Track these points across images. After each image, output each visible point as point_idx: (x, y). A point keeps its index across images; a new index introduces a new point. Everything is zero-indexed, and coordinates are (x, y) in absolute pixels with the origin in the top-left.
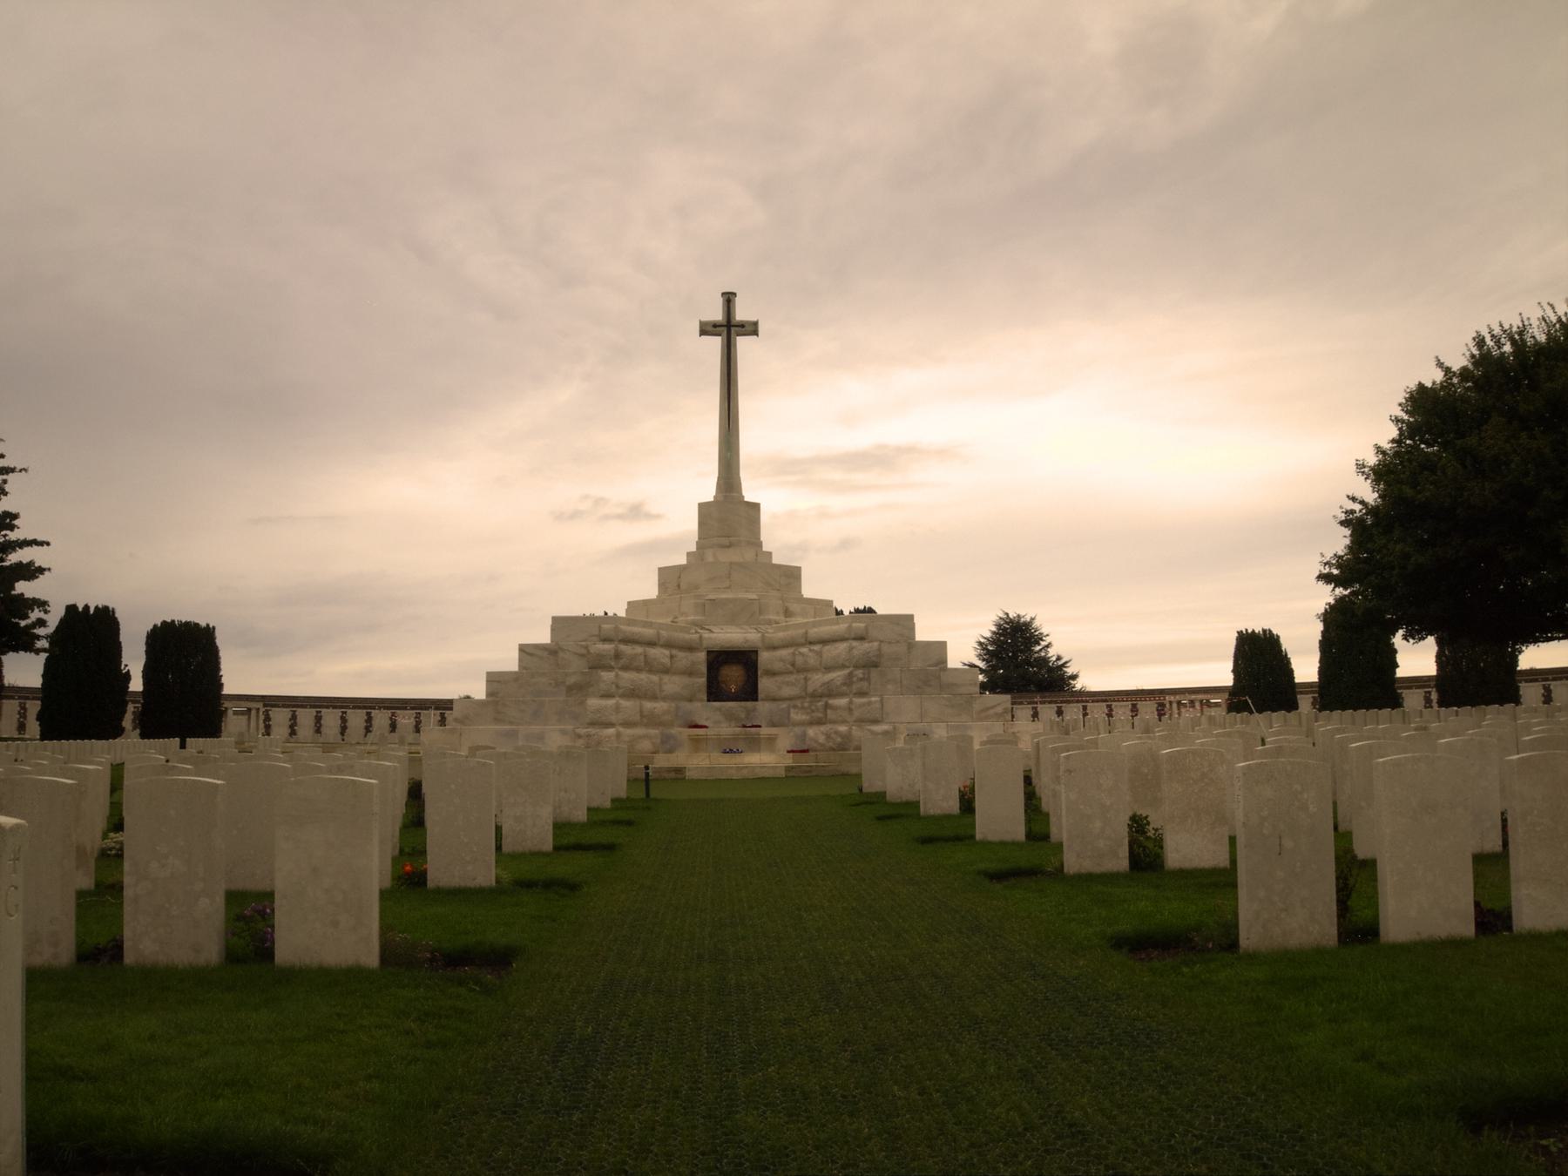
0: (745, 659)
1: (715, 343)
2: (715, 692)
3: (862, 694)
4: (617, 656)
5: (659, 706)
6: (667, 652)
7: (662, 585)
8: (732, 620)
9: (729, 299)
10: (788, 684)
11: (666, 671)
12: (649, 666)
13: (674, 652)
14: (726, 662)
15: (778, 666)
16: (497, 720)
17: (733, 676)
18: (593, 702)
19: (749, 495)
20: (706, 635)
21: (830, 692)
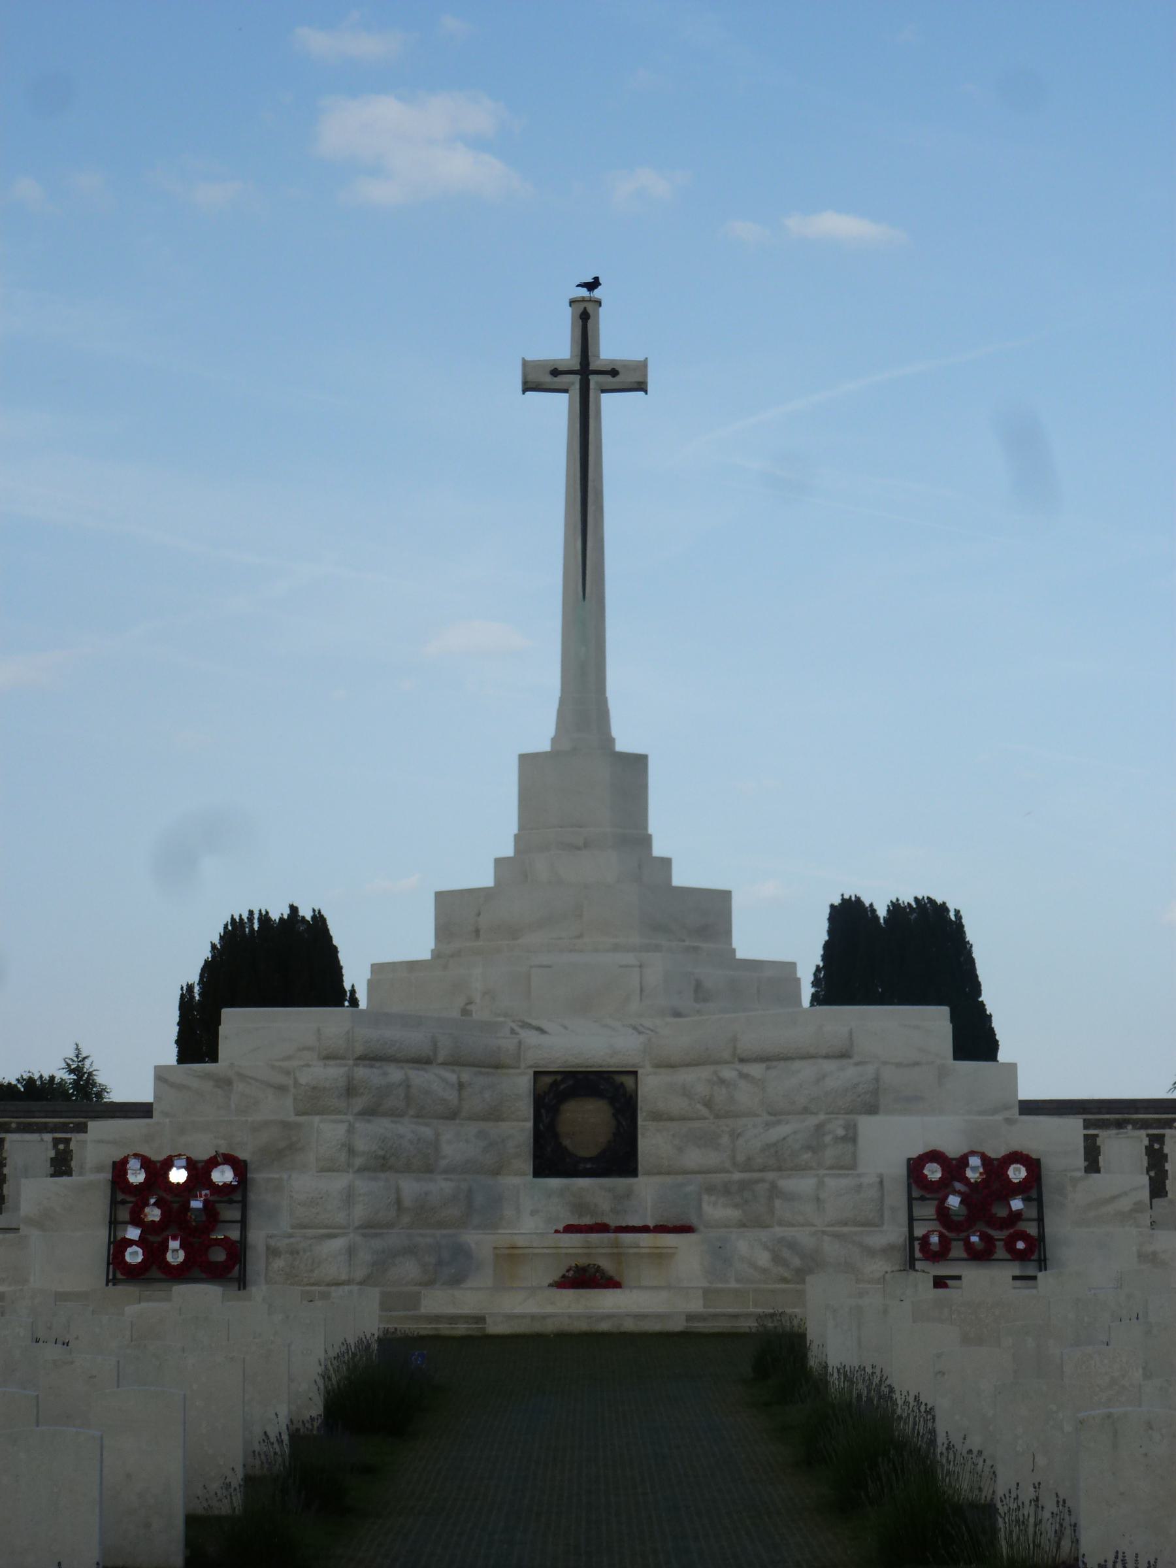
1: (557, 408)
2: (551, 1158)
4: (350, 1090)
6: (452, 1077)
7: (444, 930)
9: (585, 318)
13: (466, 1075)
19: (627, 737)
20: (531, 1038)
21: (780, 1160)
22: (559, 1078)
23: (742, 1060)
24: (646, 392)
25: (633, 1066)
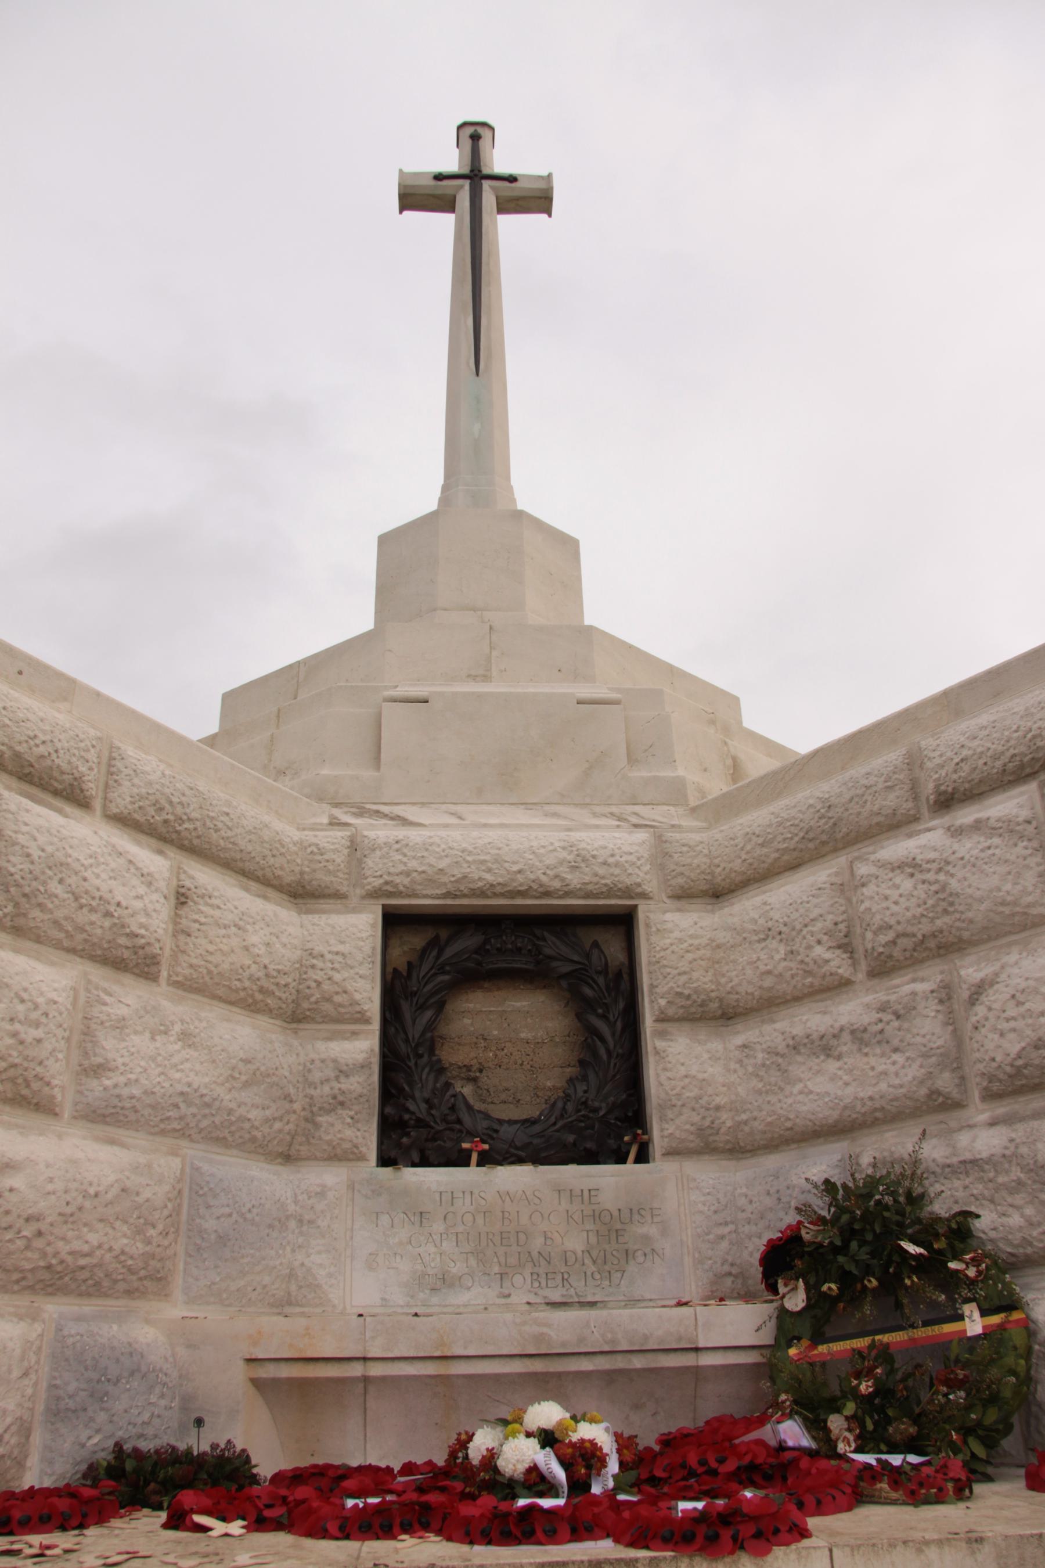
1: (441, 229)
8: (505, 778)
10: (824, 1046)
11: (129, 959)
13: (203, 876)
14: (474, 976)
15: (744, 973)
17: (512, 1038)
20: (379, 832)
22: (444, 934)
23: (947, 801)
24: (550, 216)
25: (628, 892)
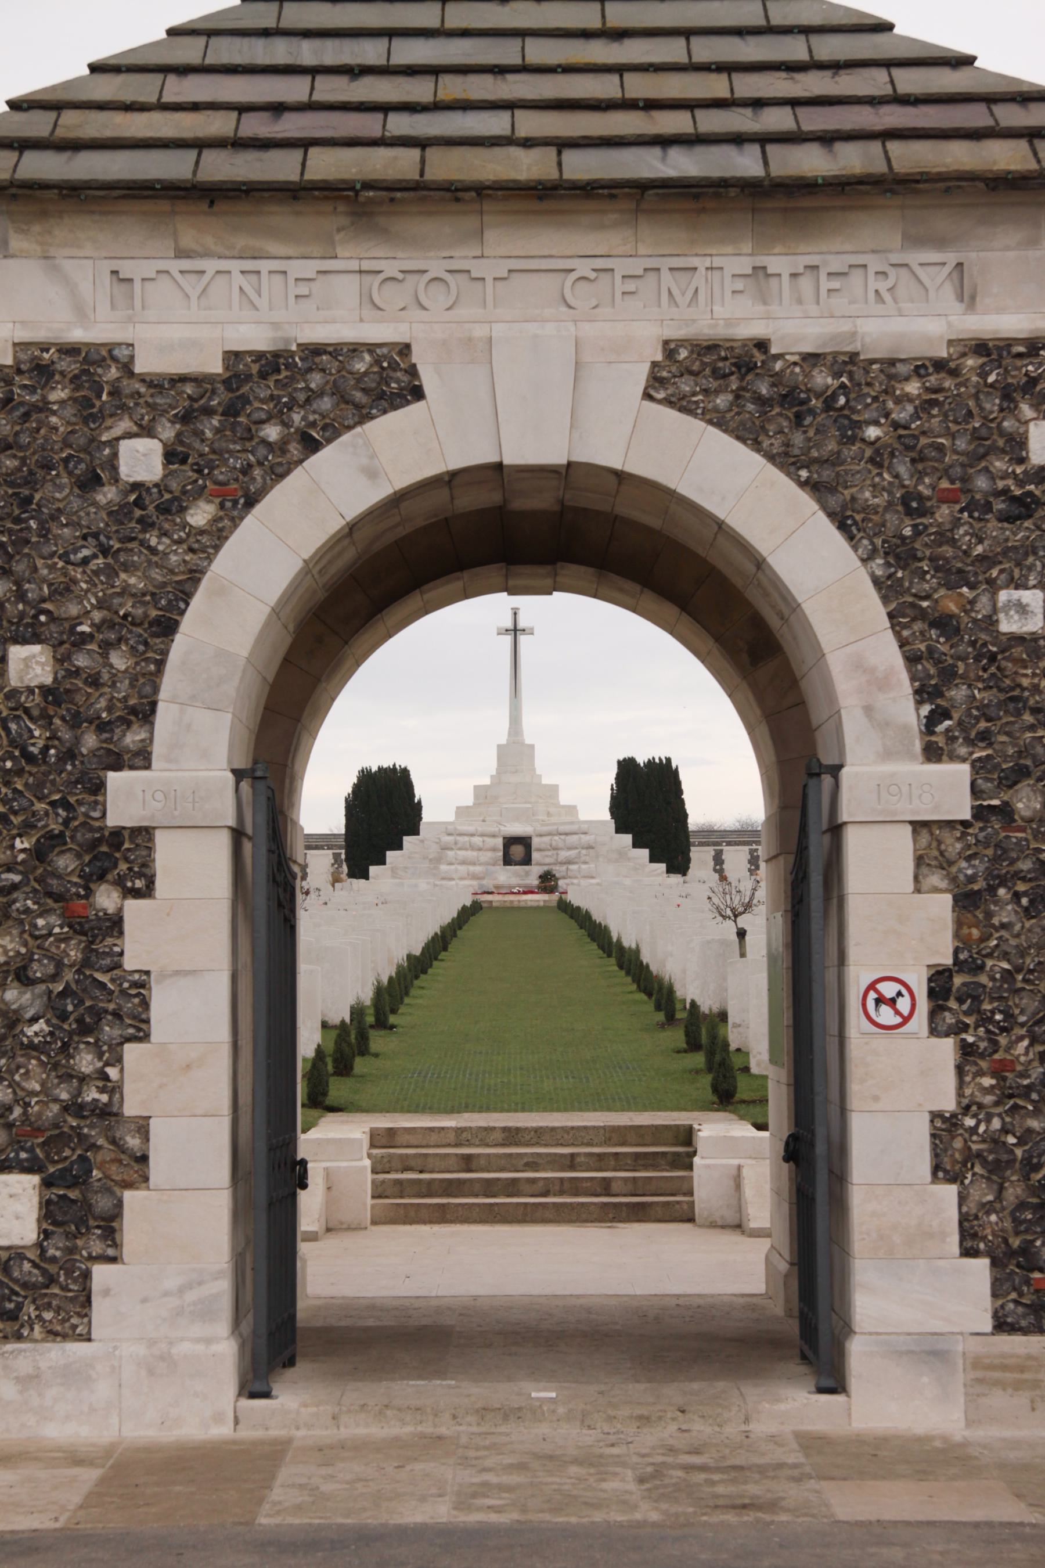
0: (525, 842)
2: (507, 861)
3: (585, 863)
4: (456, 843)
5: (478, 869)
7: (476, 796)
11: (480, 849)
12: (473, 847)
15: (543, 846)
16: (394, 877)
17: (517, 851)
18: (444, 867)
